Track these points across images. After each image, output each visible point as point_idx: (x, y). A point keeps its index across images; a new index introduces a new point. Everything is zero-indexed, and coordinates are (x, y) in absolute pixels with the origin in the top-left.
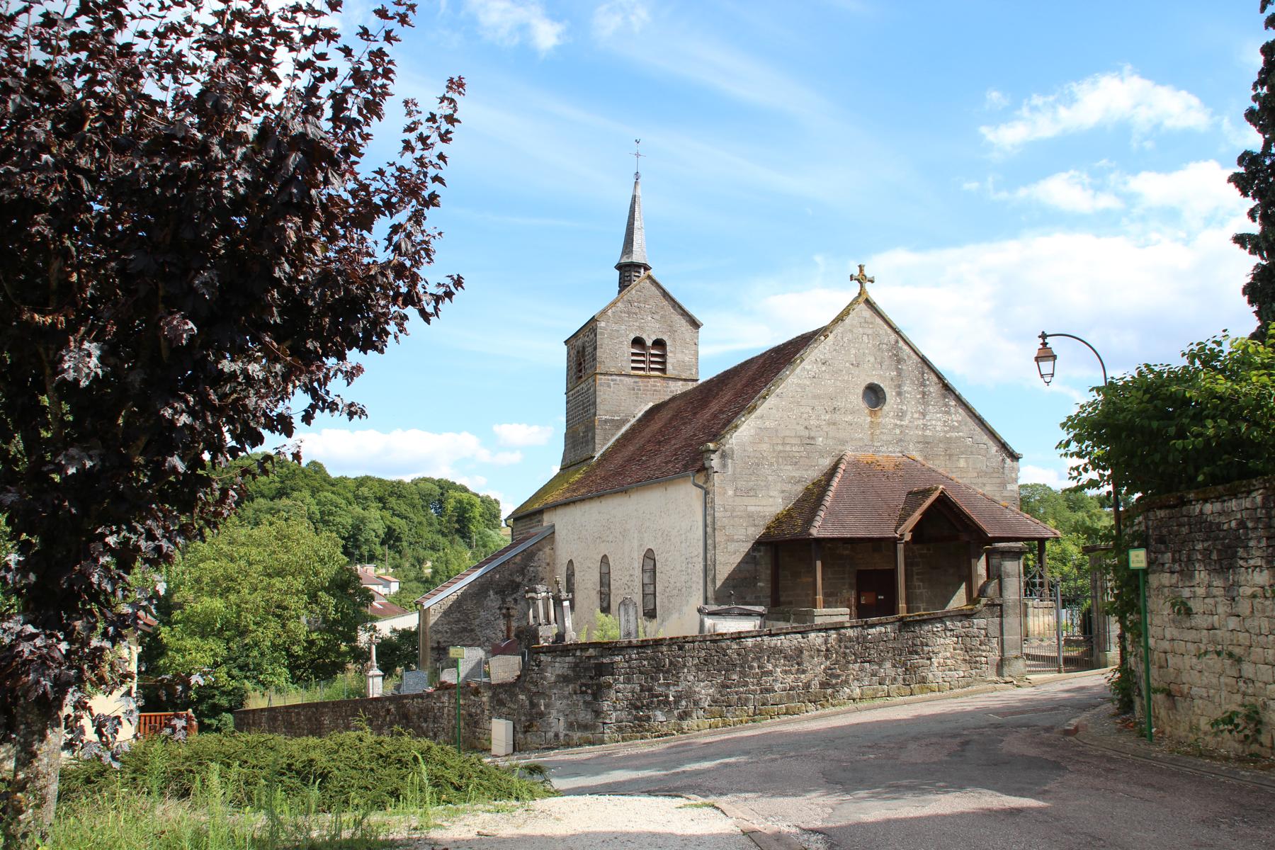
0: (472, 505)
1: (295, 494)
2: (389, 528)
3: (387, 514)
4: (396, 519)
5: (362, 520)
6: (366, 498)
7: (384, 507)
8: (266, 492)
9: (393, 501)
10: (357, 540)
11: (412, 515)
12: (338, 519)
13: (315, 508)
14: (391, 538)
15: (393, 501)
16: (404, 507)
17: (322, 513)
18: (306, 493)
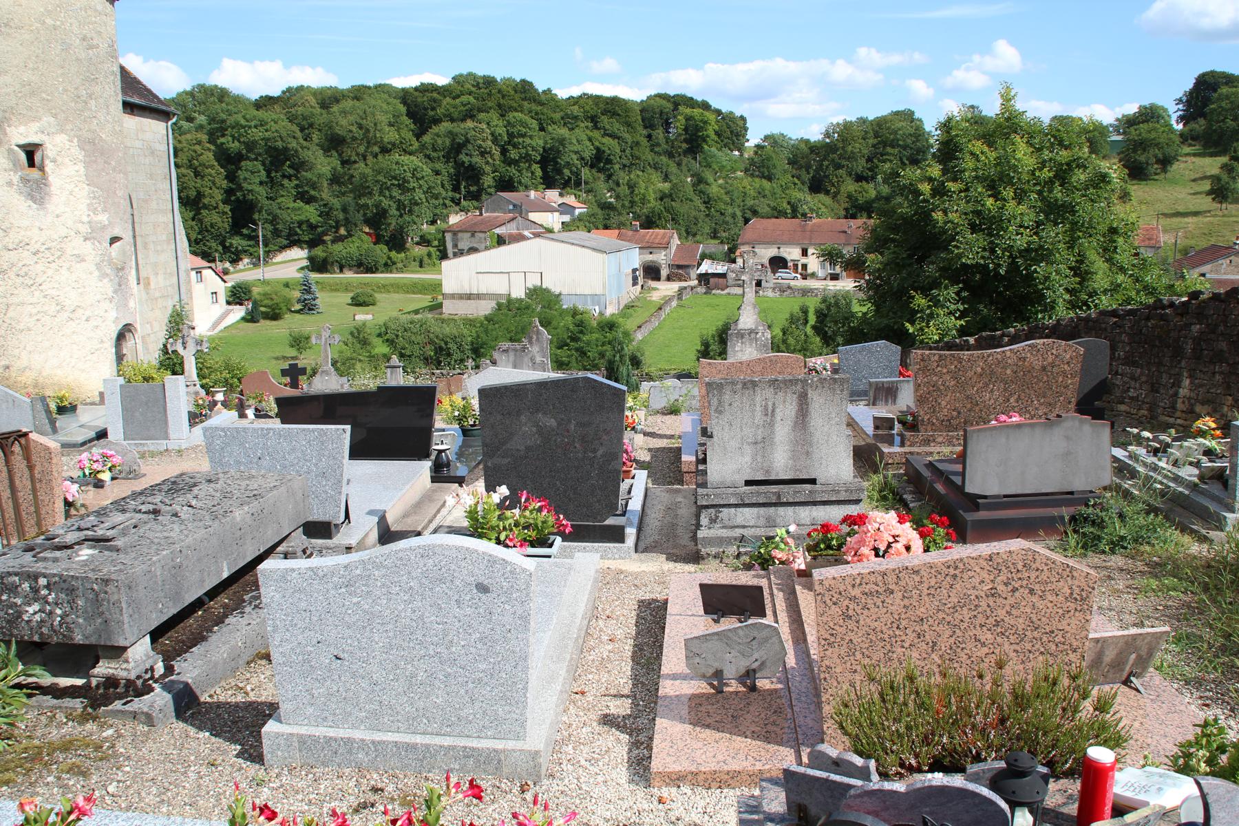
0: (706, 123)
1: (482, 116)
2: (598, 149)
3: (596, 134)
4: (607, 140)
5: (562, 141)
6: (576, 118)
7: (596, 127)
8: (456, 115)
9: (605, 121)
10: (557, 163)
11: (626, 135)
12: (528, 141)
13: (501, 130)
14: (600, 161)
15: (605, 121)
16: (617, 125)
17: (511, 135)
18: (494, 116)
